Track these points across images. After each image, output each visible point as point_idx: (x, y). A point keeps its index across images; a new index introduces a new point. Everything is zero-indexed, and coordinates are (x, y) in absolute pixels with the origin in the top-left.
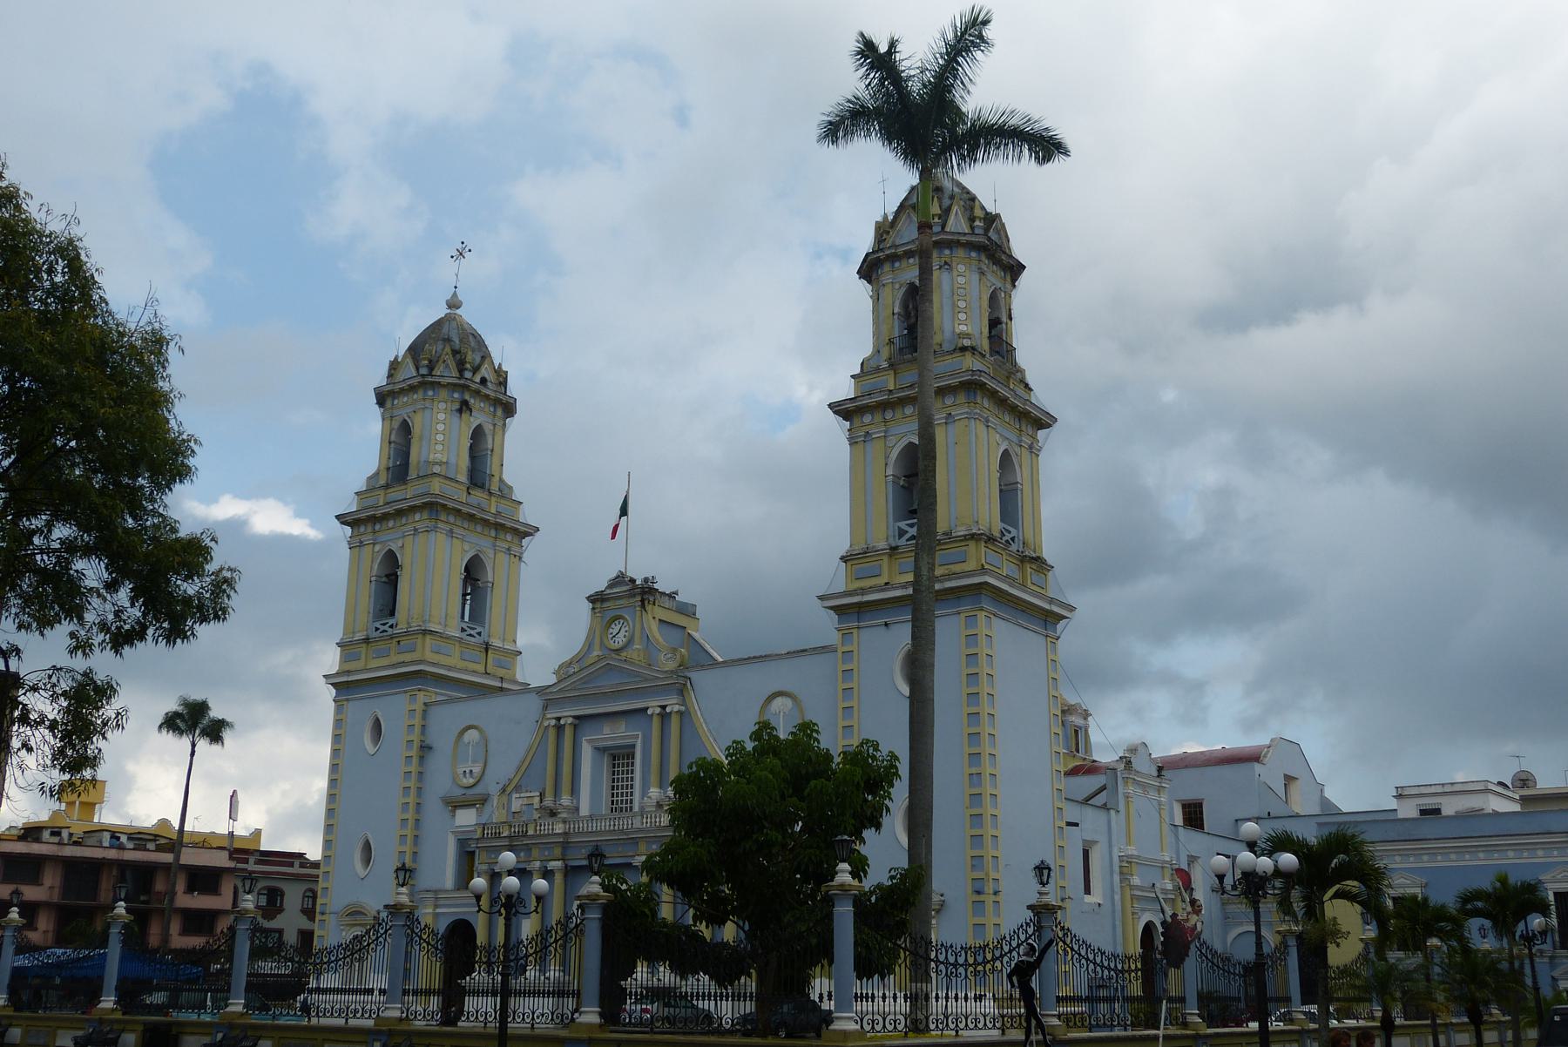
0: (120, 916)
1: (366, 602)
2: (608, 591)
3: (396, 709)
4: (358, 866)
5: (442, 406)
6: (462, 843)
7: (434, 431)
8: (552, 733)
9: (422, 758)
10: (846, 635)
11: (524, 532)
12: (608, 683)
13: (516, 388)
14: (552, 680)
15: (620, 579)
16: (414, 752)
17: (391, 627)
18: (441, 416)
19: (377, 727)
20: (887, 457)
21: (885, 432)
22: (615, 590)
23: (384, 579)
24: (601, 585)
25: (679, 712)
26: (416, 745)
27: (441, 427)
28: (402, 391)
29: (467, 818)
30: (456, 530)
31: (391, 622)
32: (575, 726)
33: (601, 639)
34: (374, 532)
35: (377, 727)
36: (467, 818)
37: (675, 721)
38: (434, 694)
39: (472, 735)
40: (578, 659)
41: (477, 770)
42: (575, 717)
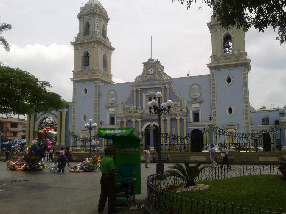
0: (152, 127)
1: (80, 63)
2: (148, 62)
3: (91, 87)
4: (83, 121)
5: (97, 19)
6: (110, 115)
7: (95, 24)
8: (135, 92)
9: (99, 97)
10: (212, 73)
11: (112, 49)
12: (150, 83)
13: (109, 16)
14: (133, 81)
15: (151, 60)
16: (97, 96)
17: (88, 68)
18: (97, 21)
19: (86, 91)
20: (221, 35)
21: (221, 30)
22: (149, 62)
23: (84, 57)
24: (147, 61)
25: (169, 88)
26: (97, 94)
27: (97, 23)
28: (86, 15)
29: (112, 110)
30: (102, 47)
31: (88, 67)
32: (141, 91)
33: (147, 71)
34: (81, 46)
35: (86, 91)
36: (112, 110)
37: (168, 90)
38: (99, 83)
39: (112, 92)
40: (141, 76)
41: (114, 100)
42: (141, 89)
